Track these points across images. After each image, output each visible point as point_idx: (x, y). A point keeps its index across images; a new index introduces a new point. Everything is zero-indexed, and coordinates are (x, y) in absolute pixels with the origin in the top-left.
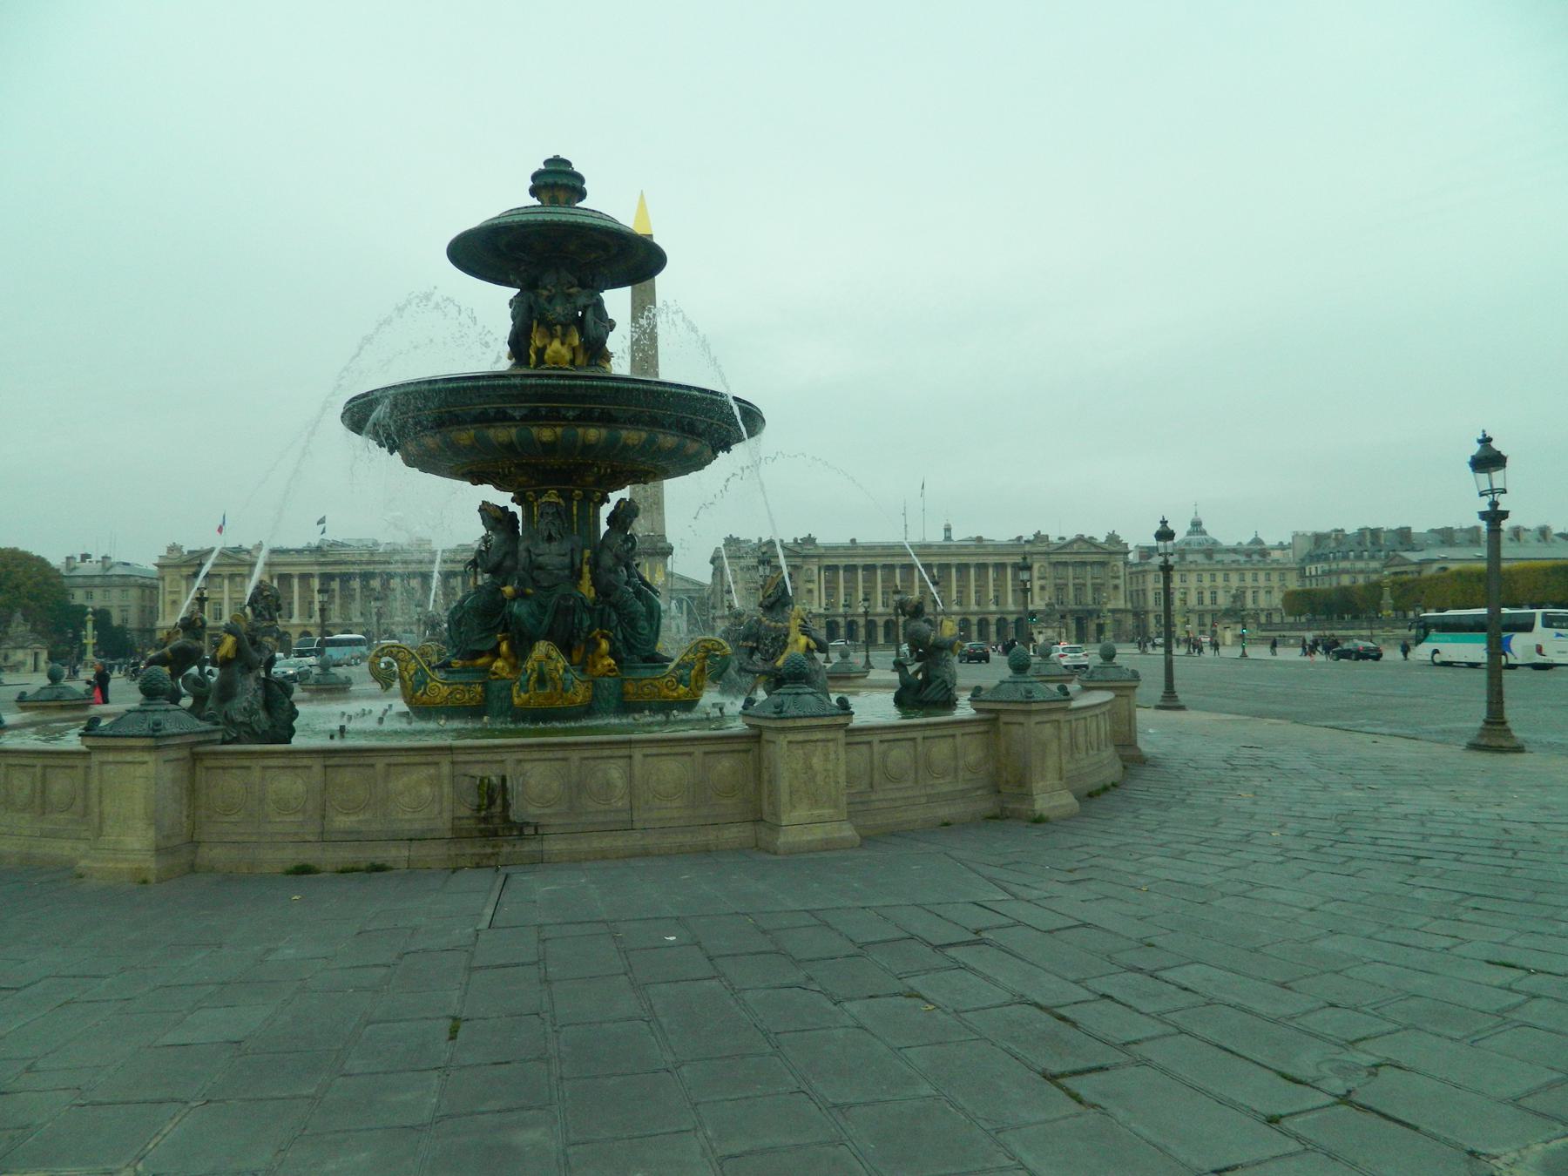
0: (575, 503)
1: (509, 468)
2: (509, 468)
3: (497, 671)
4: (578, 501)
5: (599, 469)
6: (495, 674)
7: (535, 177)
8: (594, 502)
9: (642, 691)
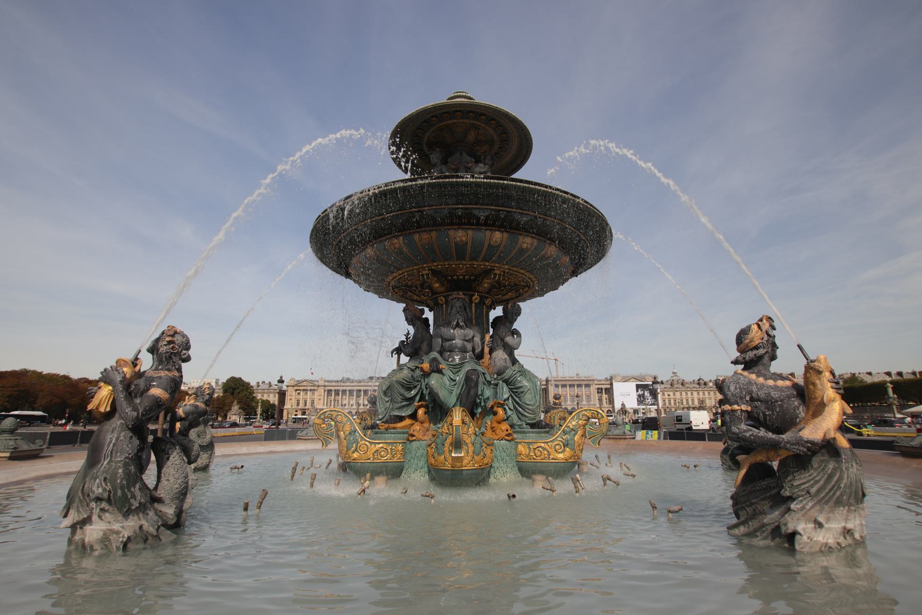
0: (473, 305)
3: (415, 433)
4: (476, 304)
5: (495, 275)
8: (487, 306)
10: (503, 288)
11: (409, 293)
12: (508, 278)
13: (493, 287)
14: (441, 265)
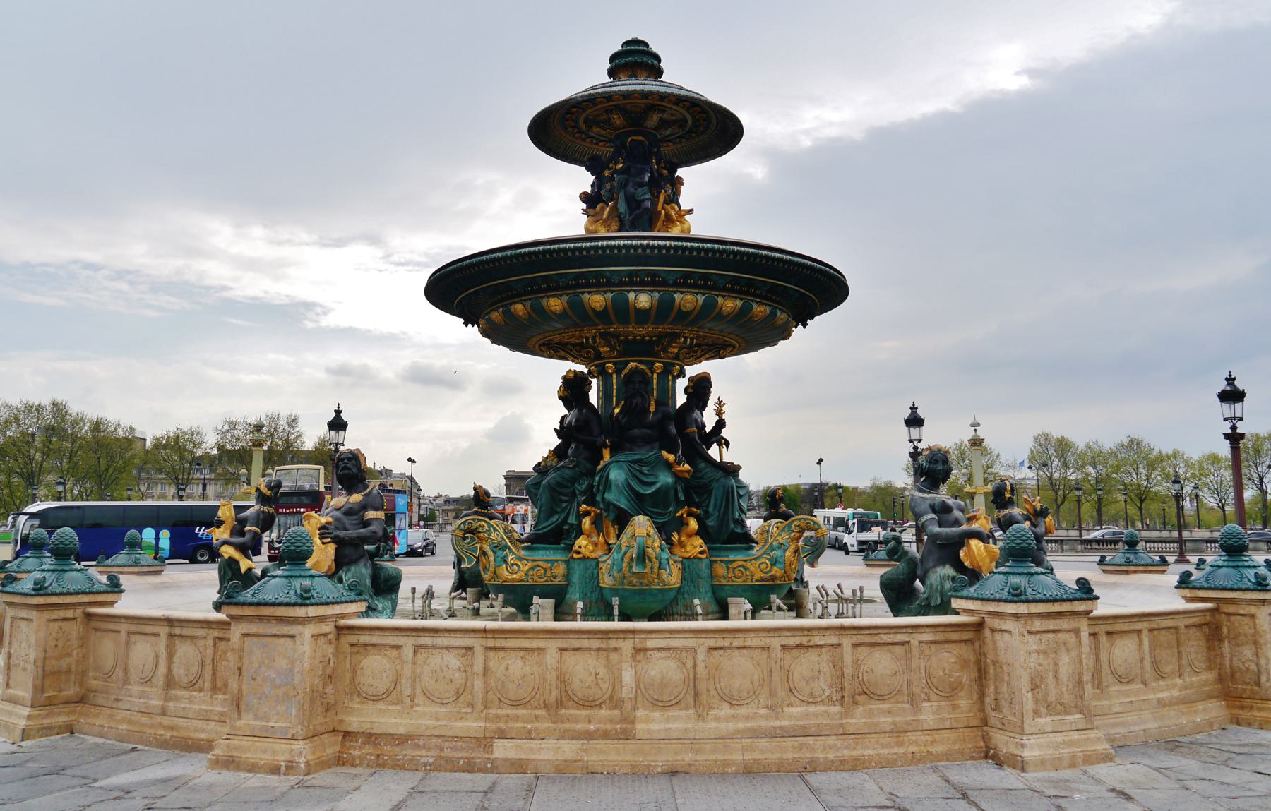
0: (655, 376)
1: (594, 338)
2: (594, 338)
3: (583, 550)
4: (658, 374)
5: (686, 338)
6: (578, 553)
7: (612, 59)
9: (734, 574)
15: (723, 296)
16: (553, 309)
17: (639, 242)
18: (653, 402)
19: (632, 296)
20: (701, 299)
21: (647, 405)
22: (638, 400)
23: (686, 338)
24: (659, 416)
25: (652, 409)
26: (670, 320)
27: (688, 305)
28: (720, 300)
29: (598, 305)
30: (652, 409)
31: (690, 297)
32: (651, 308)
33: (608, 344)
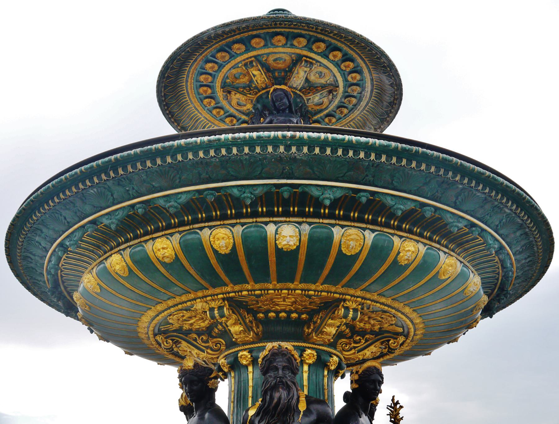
0: (306, 368)
1: (220, 308)
2: (220, 308)
4: (310, 365)
5: (347, 309)
8: (329, 371)
10: (358, 338)
11: (184, 344)
12: (369, 318)
13: (340, 335)
14: (248, 291)
15: (401, 237)
16: (160, 254)
17: (280, 134)
18: (303, 399)
19: (271, 229)
20: (370, 237)
21: (294, 401)
22: (281, 394)
23: (347, 309)
24: (313, 417)
25: (302, 407)
26: (326, 272)
27: (352, 243)
28: (396, 241)
29: (223, 243)
30: (302, 407)
31: (353, 231)
32: (298, 247)
33: (241, 321)
